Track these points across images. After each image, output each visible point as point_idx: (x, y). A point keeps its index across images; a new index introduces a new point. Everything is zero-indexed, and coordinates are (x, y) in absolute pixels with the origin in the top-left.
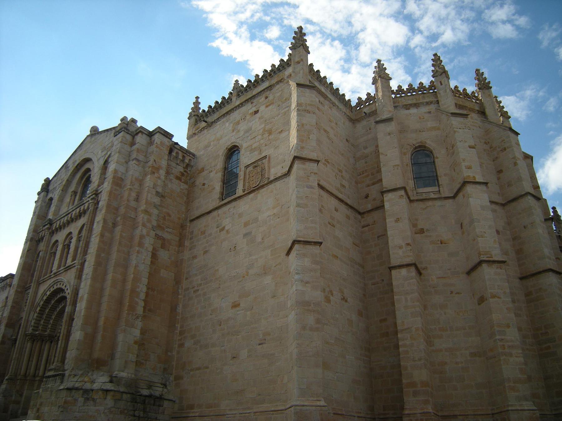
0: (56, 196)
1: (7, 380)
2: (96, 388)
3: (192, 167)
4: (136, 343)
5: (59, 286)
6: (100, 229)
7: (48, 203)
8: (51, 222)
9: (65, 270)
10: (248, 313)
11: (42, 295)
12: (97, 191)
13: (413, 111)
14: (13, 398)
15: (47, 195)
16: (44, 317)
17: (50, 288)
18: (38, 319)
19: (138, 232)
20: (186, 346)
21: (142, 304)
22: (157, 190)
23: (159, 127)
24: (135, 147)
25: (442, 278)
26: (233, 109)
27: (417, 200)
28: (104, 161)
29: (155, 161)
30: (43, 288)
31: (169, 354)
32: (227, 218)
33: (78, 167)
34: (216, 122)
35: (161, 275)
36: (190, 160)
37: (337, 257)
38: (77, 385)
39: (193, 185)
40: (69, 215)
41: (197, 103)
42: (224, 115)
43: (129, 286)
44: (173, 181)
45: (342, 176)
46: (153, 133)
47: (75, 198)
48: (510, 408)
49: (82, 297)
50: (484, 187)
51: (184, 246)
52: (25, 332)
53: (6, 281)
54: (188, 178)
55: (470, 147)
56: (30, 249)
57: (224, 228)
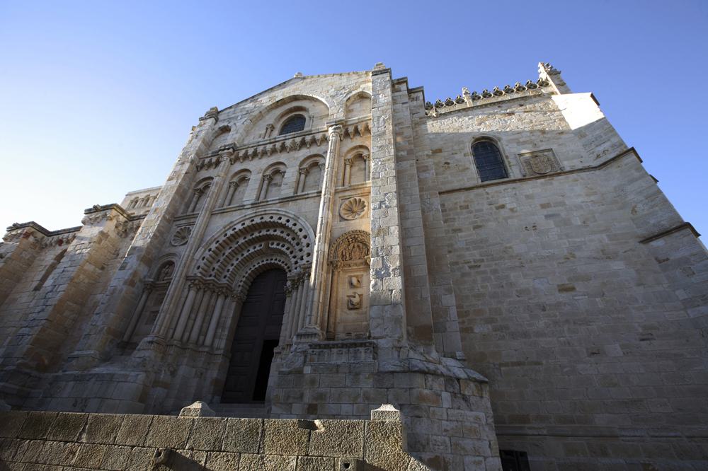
7: (216, 132)
11: (224, 228)
17: (244, 220)
18: (211, 259)
33: (280, 103)
52: (187, 272)
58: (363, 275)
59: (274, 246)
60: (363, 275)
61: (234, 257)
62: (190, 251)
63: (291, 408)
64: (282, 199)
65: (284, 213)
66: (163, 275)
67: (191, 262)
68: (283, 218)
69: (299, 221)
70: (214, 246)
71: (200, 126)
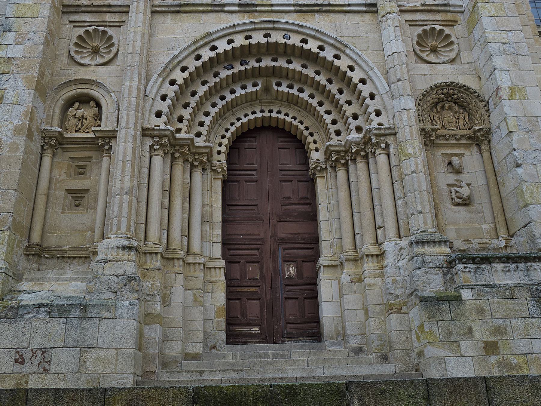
9: (298, 8)
11: (194, 43)
52: (142, 124)
58: (464, 154)
59: (284, 88)
60: (464, 154)
61: (206, 99)
62: (140, 80)
63: (459, 347)
64: (300, 5)
65: (313, 33)
66: (73, 122)
67: (144, 101)
68: (310, 40)
69: (348, 51)
70: (180, 77)
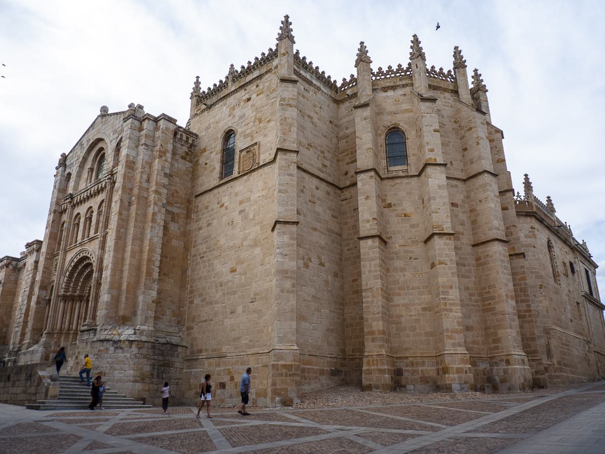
0: (74, 171)
1: (46, 334)
2: (123, 339)
3: (196, 146)
4: (153, 302)
5: (84, 255)
6: (118, 208)
7: (67, 178)
8: (72, 197)
10: (243, 277)
12: (112, 171)
13: (390, 93)
14: (53, 348)
15: (65, 170)
16: (74, 280)
18: (68, 282)
19: (151, 210)
20: (195, 302)
21: (157, 270)
22: (166, 172)
23: (164, 114)
24: (144, 132)
25: (404, 246)
26: (229, 94)
27: (388, 178)
28: (116, 143)
29: (162, 145)
30: (69, 256)
31: (182, 309)
32: (225, 196)
34: (215, 105)
35: (173, 244)
36: (193, 140)
37: (317, 229)
38: (108, 337)
39: (197, 164)
40: (89, 191)
41: (197, 83)
42: (221, 99)
43: (145, 256)
44: (179, 161)
45: (324, 157)
46: (159, 119)
47: (92, 174)
48: (446, 352)
49: (107, 266)
50: (443, 168)
51: (191, 218)
52: (58, 293)
53: (32, 247)
54: (193, 156)
55: (435, 131)
56: (54, 220)
57: (223, 204)
71: (57, 173)
